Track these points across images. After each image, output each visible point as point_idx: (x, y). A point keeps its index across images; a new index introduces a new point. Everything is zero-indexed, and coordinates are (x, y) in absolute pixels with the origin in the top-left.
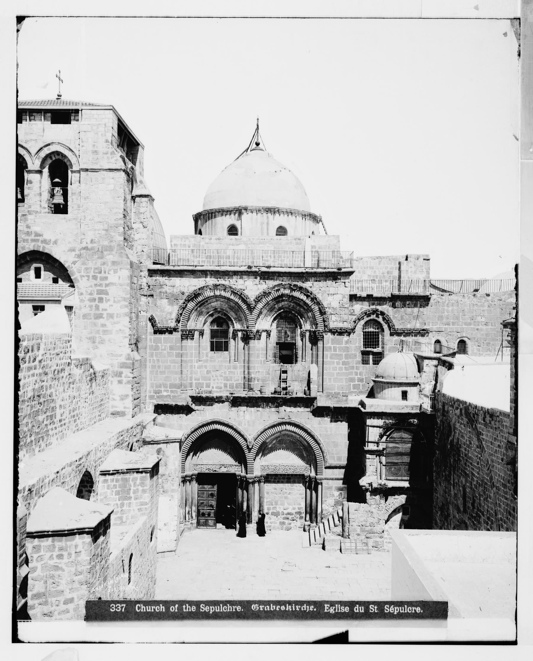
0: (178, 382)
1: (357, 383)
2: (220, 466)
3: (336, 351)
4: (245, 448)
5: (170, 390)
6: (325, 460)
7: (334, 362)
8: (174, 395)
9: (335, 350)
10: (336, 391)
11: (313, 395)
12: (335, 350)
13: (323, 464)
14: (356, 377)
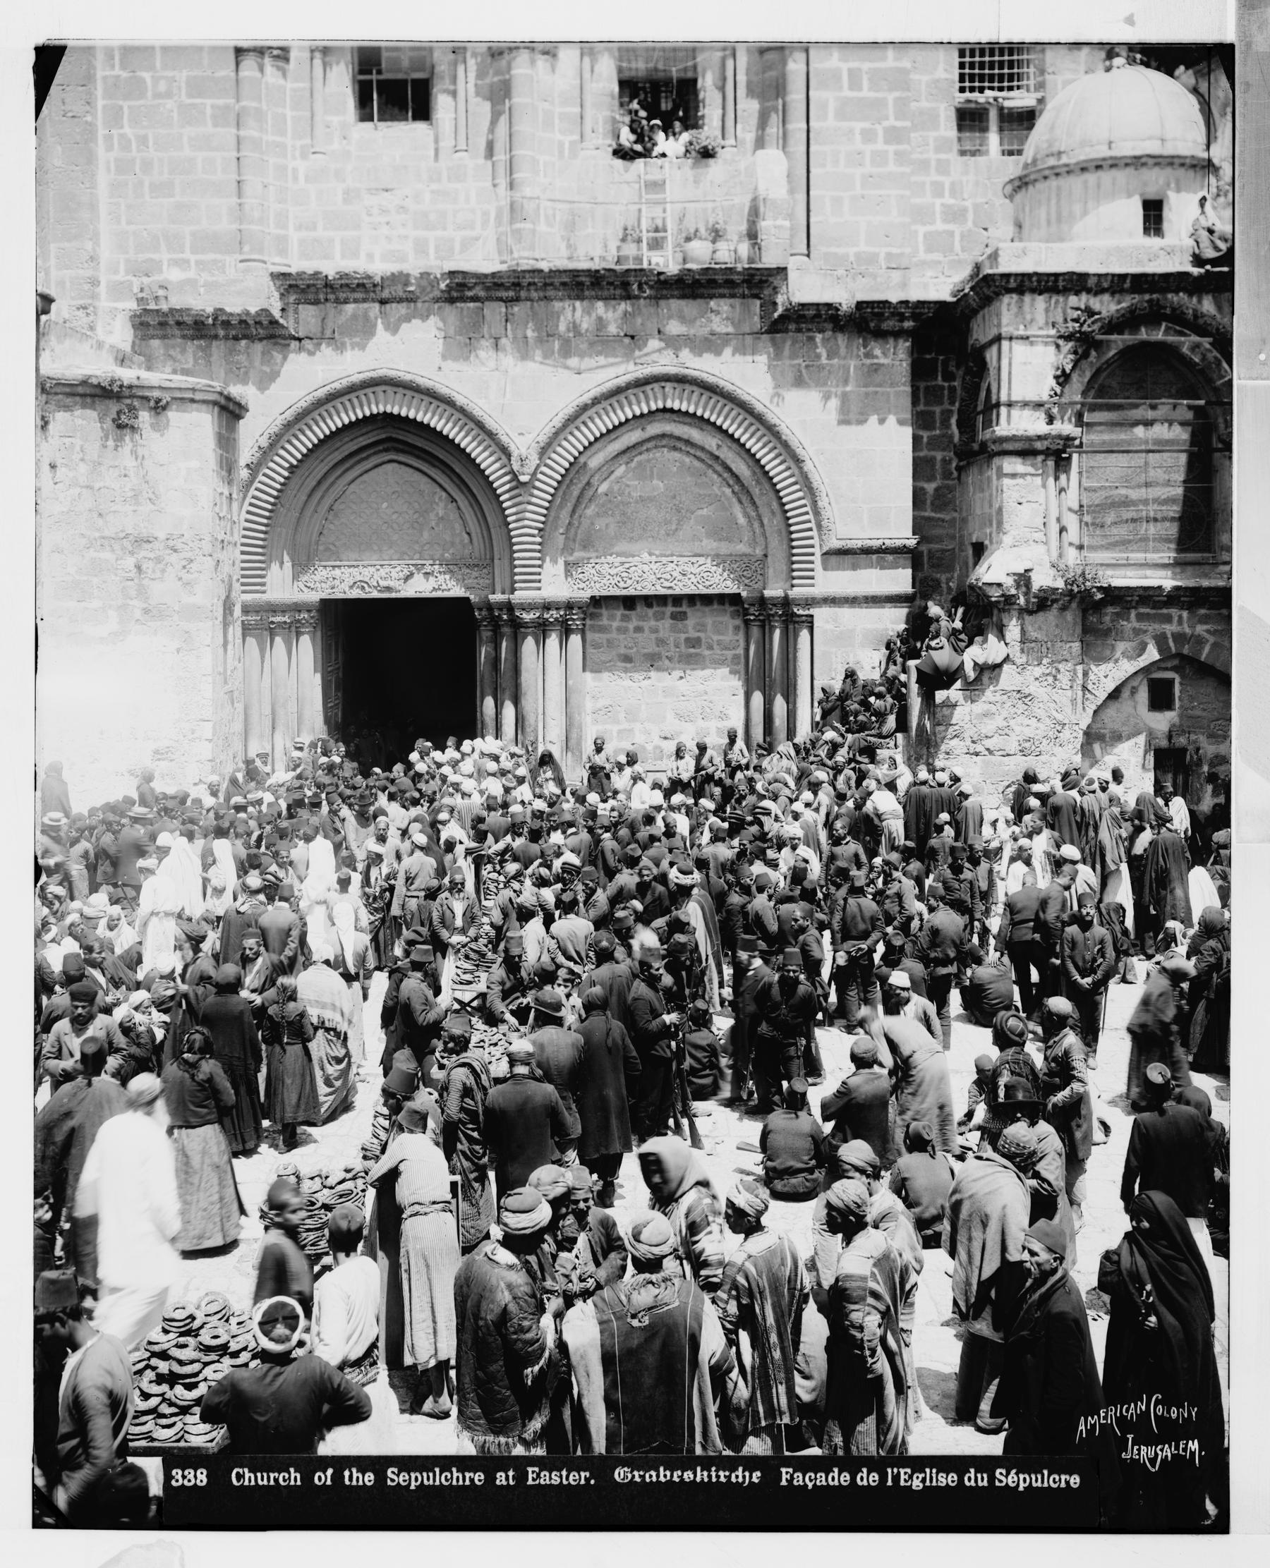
0: (225, 225)
1: (940, 226)
2: (406, 572)
3: (860, 89)
4: (501, 484)
5: (193, 258)
6: (824, 523)
7: (851, 131)
8: (210, 279)
9: (855, 83)
10: (863, 247)
11: (769, 260)
12: (855, 83)
13: (816, 542)
14: (938, 202)
